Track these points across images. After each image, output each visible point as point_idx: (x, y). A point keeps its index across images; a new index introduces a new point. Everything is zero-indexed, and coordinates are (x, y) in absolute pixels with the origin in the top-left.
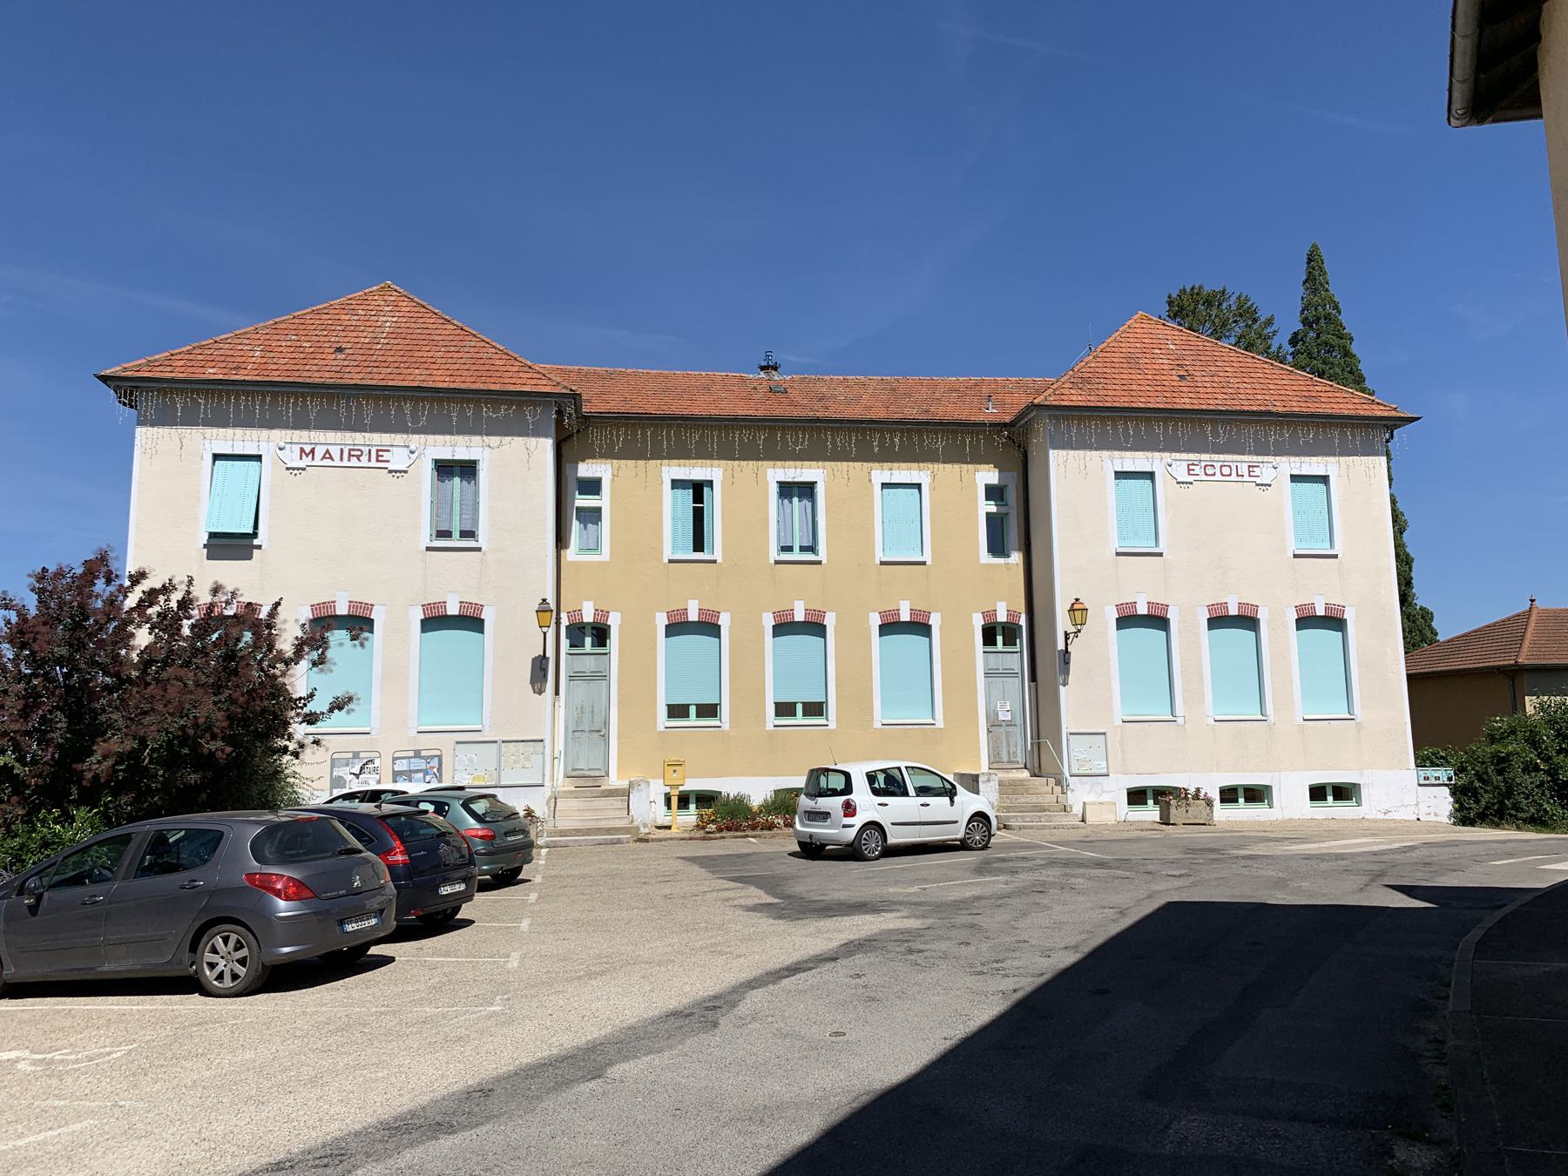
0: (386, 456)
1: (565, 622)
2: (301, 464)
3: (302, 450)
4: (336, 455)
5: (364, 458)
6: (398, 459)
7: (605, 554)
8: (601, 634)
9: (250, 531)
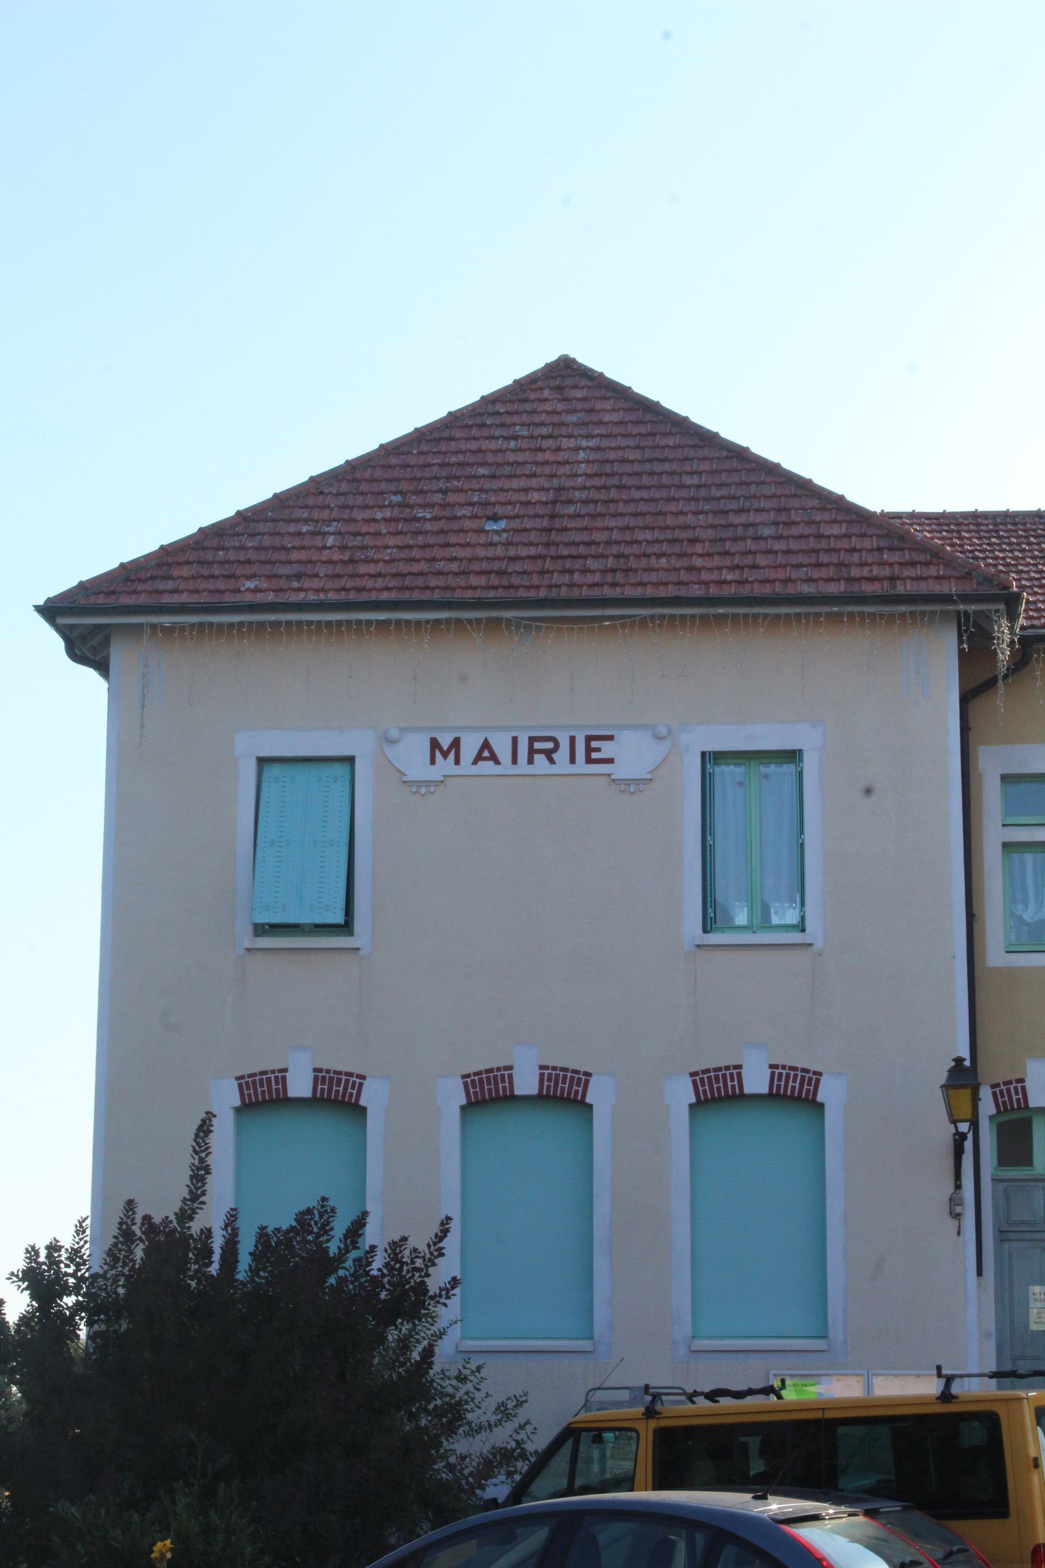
0: (607, 749)
1: (987, 1107)
3: (435, 744)
4: (503, 751)
5: (562, 755)
6: (632, 754)
9: (339, 918)
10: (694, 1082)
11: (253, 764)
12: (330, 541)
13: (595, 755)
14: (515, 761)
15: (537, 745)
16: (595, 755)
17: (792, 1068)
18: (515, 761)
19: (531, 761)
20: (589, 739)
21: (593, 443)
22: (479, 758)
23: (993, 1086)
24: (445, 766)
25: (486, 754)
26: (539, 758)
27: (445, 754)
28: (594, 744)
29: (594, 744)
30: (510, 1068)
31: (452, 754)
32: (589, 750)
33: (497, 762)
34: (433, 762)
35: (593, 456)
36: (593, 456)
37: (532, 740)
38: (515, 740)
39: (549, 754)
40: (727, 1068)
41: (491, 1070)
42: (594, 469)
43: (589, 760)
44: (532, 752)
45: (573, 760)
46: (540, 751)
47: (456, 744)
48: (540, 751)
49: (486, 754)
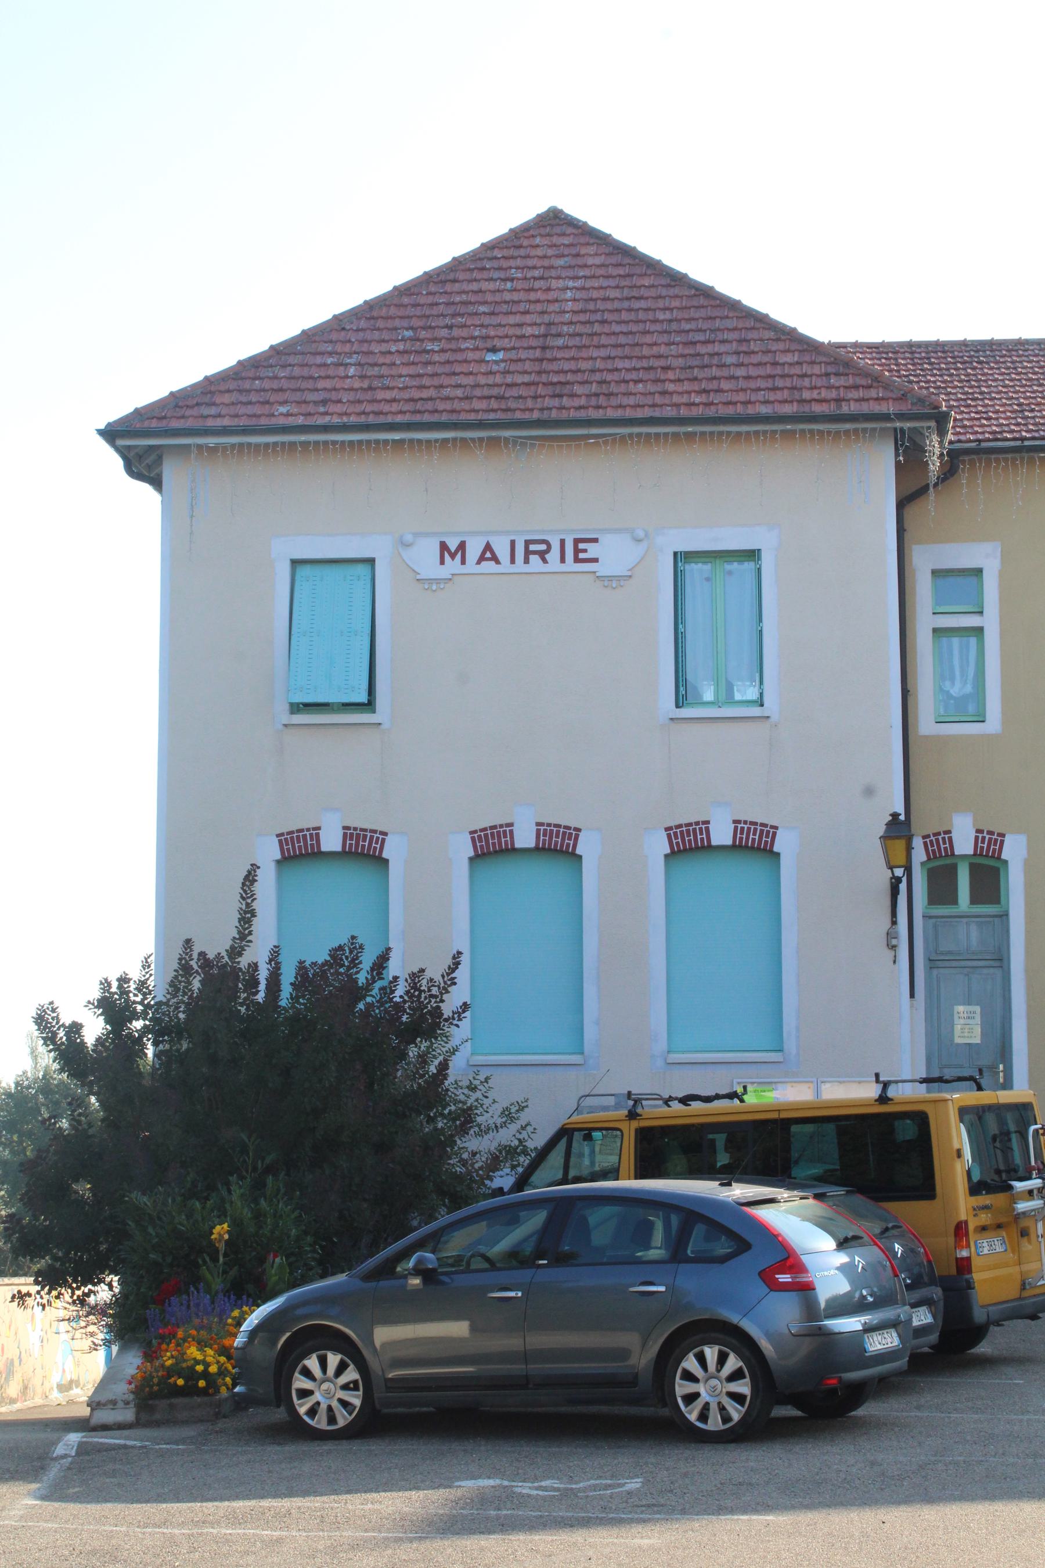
0: (592, 550)
1: (919, 855)
2: (444, 572)
3: (444, 547)
4: (503, 553)
5: (554, 555)
6: (613, 554)
7: (993, 723)
8: (988, 877)
9: (363, 698)
10: (669, 836)
11: (287, 565)
12: (352, 371)
13: (581, 556)
14: (513, 561)
15: (532, 547)
16: (581, 556)
17: (752, 823)
18: (513, 561)
19: (527, 561)
20: (577, 541)
21: (578, 283)
22: (482, 559)
23: (924, 837)
24: (453, 565)
25: (488, 555)
26: (534, 559)
27: (453, 556)
28: (581, 546)
29: (581, 546)
30: (511, 825)
31: (459, 555)
32: (577, 551)
33: (498, 562)
34: (442, 562)
35: (579, 295)
36: (579, 295)
37: (528, 543)
38: (513, 543)
39: (542, 555)
40: (697, 823)
41: (495, 827)
42: (579, 306)
43: (577, 560)
44: (528, 553)
45: (563, 560)
46: (535, 552)
47: (462, 546)
48: (535, 552)
49: (488, 555)
